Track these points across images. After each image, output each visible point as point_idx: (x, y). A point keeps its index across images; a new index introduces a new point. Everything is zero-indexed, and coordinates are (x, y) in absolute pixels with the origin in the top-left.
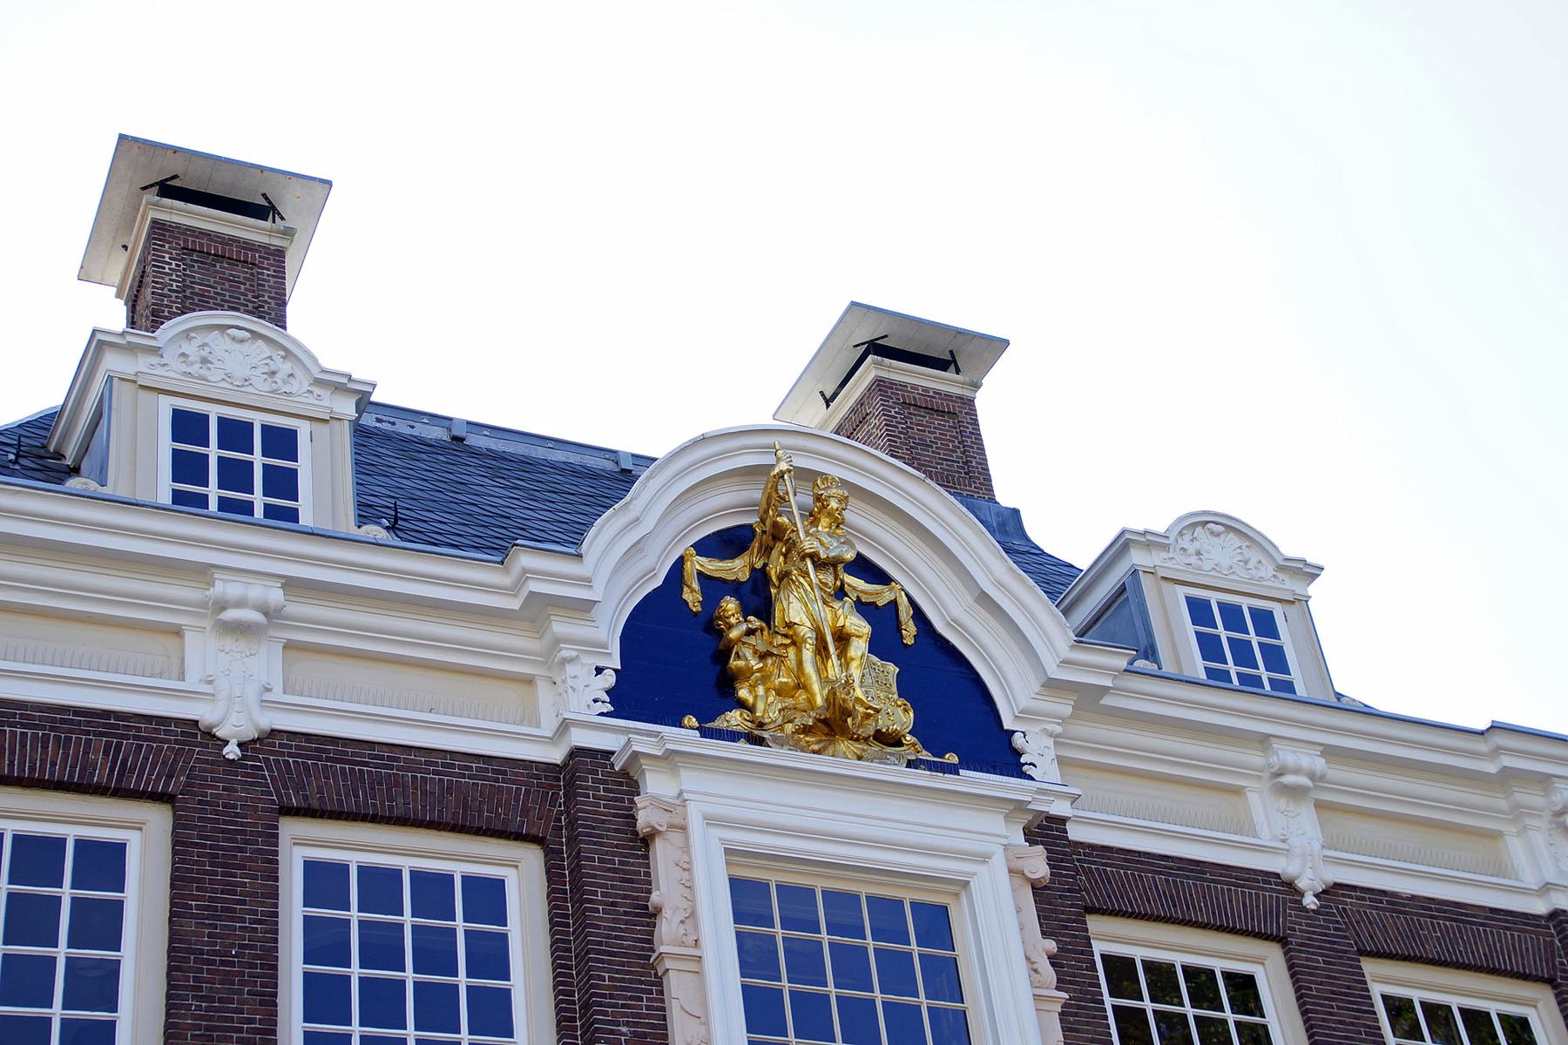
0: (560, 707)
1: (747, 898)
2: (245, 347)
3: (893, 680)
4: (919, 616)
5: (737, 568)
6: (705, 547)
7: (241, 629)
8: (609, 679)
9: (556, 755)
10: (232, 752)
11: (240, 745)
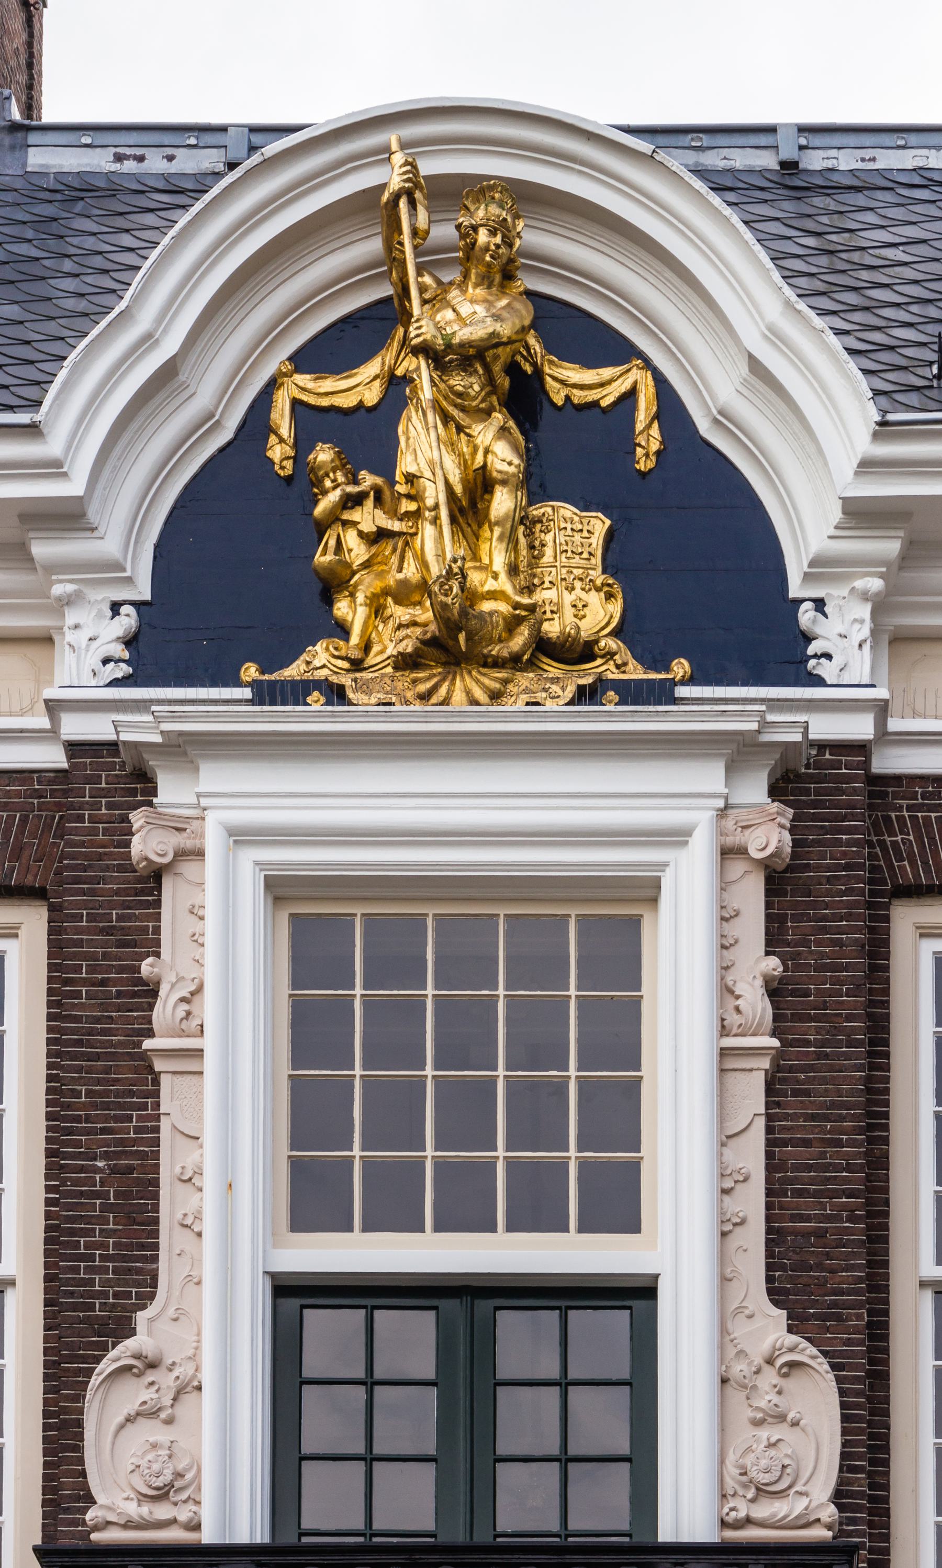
3: (597, 541)
4: (670, 408)
5: (361, 386)
6: (303, 360)
8: (128, 620)
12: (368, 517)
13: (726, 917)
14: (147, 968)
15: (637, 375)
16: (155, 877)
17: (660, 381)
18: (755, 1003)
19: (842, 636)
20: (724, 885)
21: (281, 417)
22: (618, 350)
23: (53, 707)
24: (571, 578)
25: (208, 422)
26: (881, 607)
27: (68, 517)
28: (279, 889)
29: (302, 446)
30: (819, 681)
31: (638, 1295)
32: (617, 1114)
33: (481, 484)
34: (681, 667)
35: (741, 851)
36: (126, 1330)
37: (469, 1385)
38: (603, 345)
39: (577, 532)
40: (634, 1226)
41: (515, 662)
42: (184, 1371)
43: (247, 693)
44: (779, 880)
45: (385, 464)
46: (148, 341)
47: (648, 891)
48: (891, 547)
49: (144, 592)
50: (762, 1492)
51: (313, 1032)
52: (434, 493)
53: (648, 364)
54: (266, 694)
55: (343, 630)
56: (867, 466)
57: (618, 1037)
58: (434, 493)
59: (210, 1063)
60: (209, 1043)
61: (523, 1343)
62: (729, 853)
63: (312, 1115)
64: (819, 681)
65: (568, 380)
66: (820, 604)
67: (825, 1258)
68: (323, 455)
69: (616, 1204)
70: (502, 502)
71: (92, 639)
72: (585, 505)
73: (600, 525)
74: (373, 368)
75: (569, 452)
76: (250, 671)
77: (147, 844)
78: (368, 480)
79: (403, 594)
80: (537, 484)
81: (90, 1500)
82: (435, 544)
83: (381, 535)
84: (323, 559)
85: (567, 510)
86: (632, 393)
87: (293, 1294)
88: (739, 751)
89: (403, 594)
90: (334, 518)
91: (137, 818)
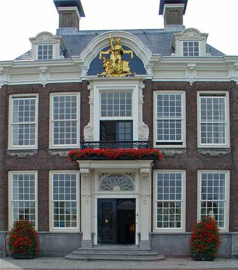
1: (103, 94)
5: (107, 52)
6: (102, 51)
7: (44, 73)
9: (81, 81)
10: (44, 86)
12: (108, 62)
13: (139, 92)
17: (133, 52)
19: (149, 71)
20: (139, 90)
21: (100, 55)
22: (130, 49)
23: (81, 78)
24: (126, 67)
25: (94, 55)
26: (152, 68)
27: (82, 63)
28: (100, 91)
29: (102, 57)
31: (131, 121)
32: (130, 107)
33: (118, 60)
34: (135, 73)
38: (128, 49)
39: (126, 63)
40: (131, 116)
41: (121, 73)
44: (143, 90)
46: (89, 50)
47: (132, 90)
48: (153, 64)
50: (142, 136)
51: (103, 102)
52: (114, 61)
54: (99, 76)
56: (151, 58)
57: (130, 101)
58: (114, 61)
59: (94, 104)
60: (94, 103)
61: (121, 125)
62: (139, 88)
63: (103, 108)
67: (148, 118)
68: (104, 58)
69: (129, 114)
70: (119, 61)
71: (84, 73)
72: (127, 61)
73: (128, 63)
74: (108, 51)
75: (125, 57)
79: (111, 68)
80: (123, 60)
81: (84, 137)
82: (114, 64)
84: (104, 65)
85: (125, 62)
88: (140, 80)
89: (111, 68)
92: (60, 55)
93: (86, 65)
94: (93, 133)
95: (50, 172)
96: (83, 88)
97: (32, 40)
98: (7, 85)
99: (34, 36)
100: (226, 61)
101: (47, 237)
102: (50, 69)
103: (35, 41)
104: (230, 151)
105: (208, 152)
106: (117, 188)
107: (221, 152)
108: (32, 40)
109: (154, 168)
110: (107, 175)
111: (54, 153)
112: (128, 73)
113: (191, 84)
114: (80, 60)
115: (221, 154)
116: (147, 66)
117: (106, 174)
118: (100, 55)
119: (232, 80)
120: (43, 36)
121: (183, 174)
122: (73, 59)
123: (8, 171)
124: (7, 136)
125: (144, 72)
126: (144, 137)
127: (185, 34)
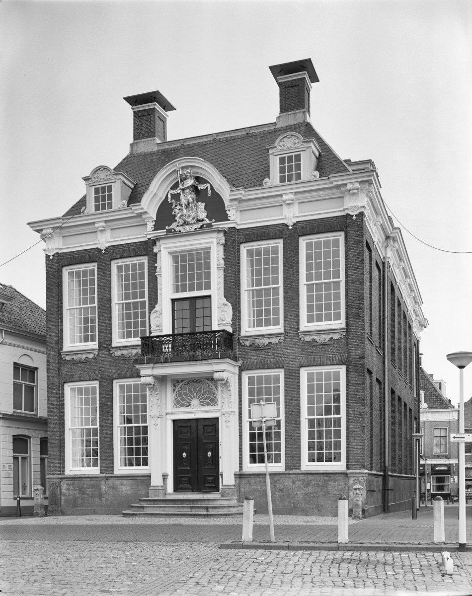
0: (148, 232)
2: (103, 171)
8: (154, 223)
9: (146, 239)
10: (104, 251)
11: (105, 250)
12: (178, 207)
14: (156, 265)
15: (208, 185)
16: (156, 254)
17: (211, 185)
18: (222, 262)
19: (232, 214)
21: (169, 196)
24: (201, 211)
25: (161, 198)
28: (170, 253)
30: (229, 220)
32: (208, 275)
34: (213, 220)
35: (219, 243)
36: (155, 307)
37: (193, 310)
39: (202, 205)
40: (210, 288)
42: (161, 312)
43: (165, 230)
44: (225, 245)
45: (179, 200)
49: (155, 219)
53: (209, 183)
55: (176, 221)
57: (208, 265)
61: (199, 304)
64: (229, 220)
65: (201, 187)
66: (229, 210)
69: (208, 287)
71: (150, 225)
72: (202, 202)
73: (204, 204)
76: (167, 228)
77: (155, 250)
78: (178, 203)
83: (180, 209)
86: (207, 187)
87: (173, 301)
90: (174, 208)
91: (154, 247)
92: (122, 199)
93: (151, 215)
94: (162, 322)
95: (115, 382)
96: (147, 249)
97: (86, 179)
98: (58, 253)
99: (88, 174)
100: (335, 183)
101: (110, 482)
102: (109, 224)
103: (90, 181)
104: (344, 334)
105: (315, 337)
106: (195, 402)
107: (331, 336)
108: (86, 179)
109: (241, 370)
110: (183, 383)
111: (118, 353)
112: (204, 222)
113: (290, 227)
114: (143, 209)
115: (331, 339)
116: (228, 206)
117: (182, 381)
118: (169, 196)
119: (347, 212)
120: (99, 172)
121: (281, 373)
122: (133, 208)
123: (64, 383)
124: (62, 330)
125: (225, 218)
126: (224, 322)
127: (281, 144)
